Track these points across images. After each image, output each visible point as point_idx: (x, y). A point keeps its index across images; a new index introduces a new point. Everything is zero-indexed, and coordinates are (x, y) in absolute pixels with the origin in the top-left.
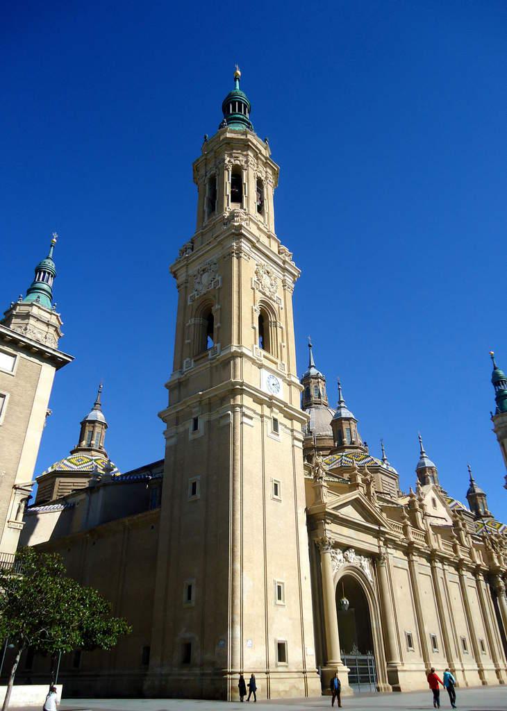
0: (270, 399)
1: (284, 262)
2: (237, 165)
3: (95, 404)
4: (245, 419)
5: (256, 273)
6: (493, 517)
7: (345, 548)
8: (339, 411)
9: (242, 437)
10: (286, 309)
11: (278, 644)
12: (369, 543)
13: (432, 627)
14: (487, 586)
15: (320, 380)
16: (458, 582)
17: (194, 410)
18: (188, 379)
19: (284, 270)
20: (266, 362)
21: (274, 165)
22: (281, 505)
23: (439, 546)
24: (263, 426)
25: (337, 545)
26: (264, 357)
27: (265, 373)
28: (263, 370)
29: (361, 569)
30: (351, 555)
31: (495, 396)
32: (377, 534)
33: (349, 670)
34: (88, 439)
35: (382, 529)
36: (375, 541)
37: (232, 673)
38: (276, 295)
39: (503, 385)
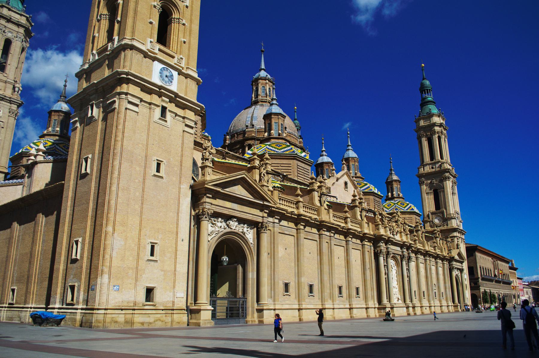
0: (160, 89)
3: (61, 96)
7: (227, 218)
8: (270, 108)
10: (192, 7)
11: (147, 289)
14: (371, 249)
15: (267, 81)
20: (160, 56)
22: (164, 180)
23: (330, 218)
24: (150, 112)
25: (216, 215)
26: (160, 50)
27: (157, 66)
30: (234, 224)
31: (420, 102)
32: (262, 208)
33: (213, 308)
34: (54, 125)
35: (266, 203)
37: (98, 309)
39: (428, 93)
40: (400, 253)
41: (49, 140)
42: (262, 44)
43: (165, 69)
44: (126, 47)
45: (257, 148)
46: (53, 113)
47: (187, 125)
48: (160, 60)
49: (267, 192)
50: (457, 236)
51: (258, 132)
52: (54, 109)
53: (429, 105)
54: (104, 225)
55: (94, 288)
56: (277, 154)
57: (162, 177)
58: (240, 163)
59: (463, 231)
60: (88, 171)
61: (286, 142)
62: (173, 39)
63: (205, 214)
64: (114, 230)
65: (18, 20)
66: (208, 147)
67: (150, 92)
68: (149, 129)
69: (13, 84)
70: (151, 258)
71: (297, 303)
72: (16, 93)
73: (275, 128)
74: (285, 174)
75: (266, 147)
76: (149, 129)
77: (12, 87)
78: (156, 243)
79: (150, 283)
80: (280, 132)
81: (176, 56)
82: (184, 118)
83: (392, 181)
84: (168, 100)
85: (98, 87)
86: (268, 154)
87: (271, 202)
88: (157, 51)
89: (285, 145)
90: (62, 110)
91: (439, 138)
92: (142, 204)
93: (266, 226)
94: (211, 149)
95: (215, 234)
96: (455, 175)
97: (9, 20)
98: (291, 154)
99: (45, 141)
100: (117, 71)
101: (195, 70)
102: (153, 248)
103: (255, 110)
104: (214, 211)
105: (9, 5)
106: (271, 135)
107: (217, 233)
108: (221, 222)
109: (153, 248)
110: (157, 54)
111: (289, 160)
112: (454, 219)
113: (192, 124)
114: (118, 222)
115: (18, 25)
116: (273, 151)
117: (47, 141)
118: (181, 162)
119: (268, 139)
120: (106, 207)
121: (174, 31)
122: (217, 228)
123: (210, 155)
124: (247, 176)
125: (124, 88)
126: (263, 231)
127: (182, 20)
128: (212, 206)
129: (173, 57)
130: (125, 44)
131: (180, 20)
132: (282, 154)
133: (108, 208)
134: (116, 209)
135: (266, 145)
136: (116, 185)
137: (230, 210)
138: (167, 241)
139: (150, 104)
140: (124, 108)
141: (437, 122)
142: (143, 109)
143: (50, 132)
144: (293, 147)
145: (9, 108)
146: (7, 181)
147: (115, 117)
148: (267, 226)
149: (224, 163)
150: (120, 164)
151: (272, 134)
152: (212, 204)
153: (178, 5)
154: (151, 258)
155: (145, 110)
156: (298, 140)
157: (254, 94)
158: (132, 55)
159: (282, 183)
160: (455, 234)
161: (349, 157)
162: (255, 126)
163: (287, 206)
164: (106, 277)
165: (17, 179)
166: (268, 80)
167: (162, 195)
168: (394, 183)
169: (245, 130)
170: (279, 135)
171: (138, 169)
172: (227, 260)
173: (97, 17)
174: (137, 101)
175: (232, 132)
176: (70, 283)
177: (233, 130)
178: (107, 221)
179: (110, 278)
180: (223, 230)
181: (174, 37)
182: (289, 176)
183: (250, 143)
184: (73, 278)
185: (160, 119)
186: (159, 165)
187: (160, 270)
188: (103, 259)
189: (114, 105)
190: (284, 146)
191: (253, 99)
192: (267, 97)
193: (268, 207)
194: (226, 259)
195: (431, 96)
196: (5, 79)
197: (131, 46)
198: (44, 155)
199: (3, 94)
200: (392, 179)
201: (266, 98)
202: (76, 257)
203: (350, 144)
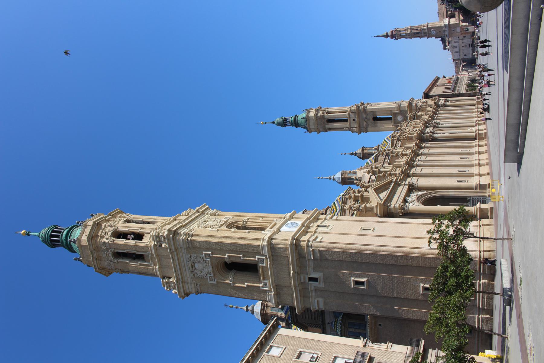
1: (197, 211)
2: (112, 234)
4: (318, 240)
5: (205, 227)
6: (379, 145)
7: (405, 201)
9: (330, 243)
12: (402, 190)
13: (455, 171)
16: (426, 156)
17: (302, 281)
18: (276, 286)
19: (203, 213)
21: (115, 211)
22: (376, 228)
28: (281, 230)
29: (418, 196)
30: (410, 199)
33: (479, 203)
35: (394, 181)
36: (400, 189)
37: (480, 257)
39: (286, 120)
40: (432, 128)
44: (270, 243)
47: (332, 218)
50: (416, 103)
53: (298, 120)
54: (413, 255)
57: (374, 229)
59: (411, 99)
71: (475, 167)
83: (363, 154)
91: (328, 113)
96: (361, 103)
98: (342, 200)
112: (400, 104)
125: (303, 243)
127: (245, 219)
134: (401, 247)
141: (314, 113)
160: (414, 104)
161: (341, 177)
168: (364, 152)
190: (334, 207)
195: (290, 118)
200: (360, 153)
203: (329, 177)
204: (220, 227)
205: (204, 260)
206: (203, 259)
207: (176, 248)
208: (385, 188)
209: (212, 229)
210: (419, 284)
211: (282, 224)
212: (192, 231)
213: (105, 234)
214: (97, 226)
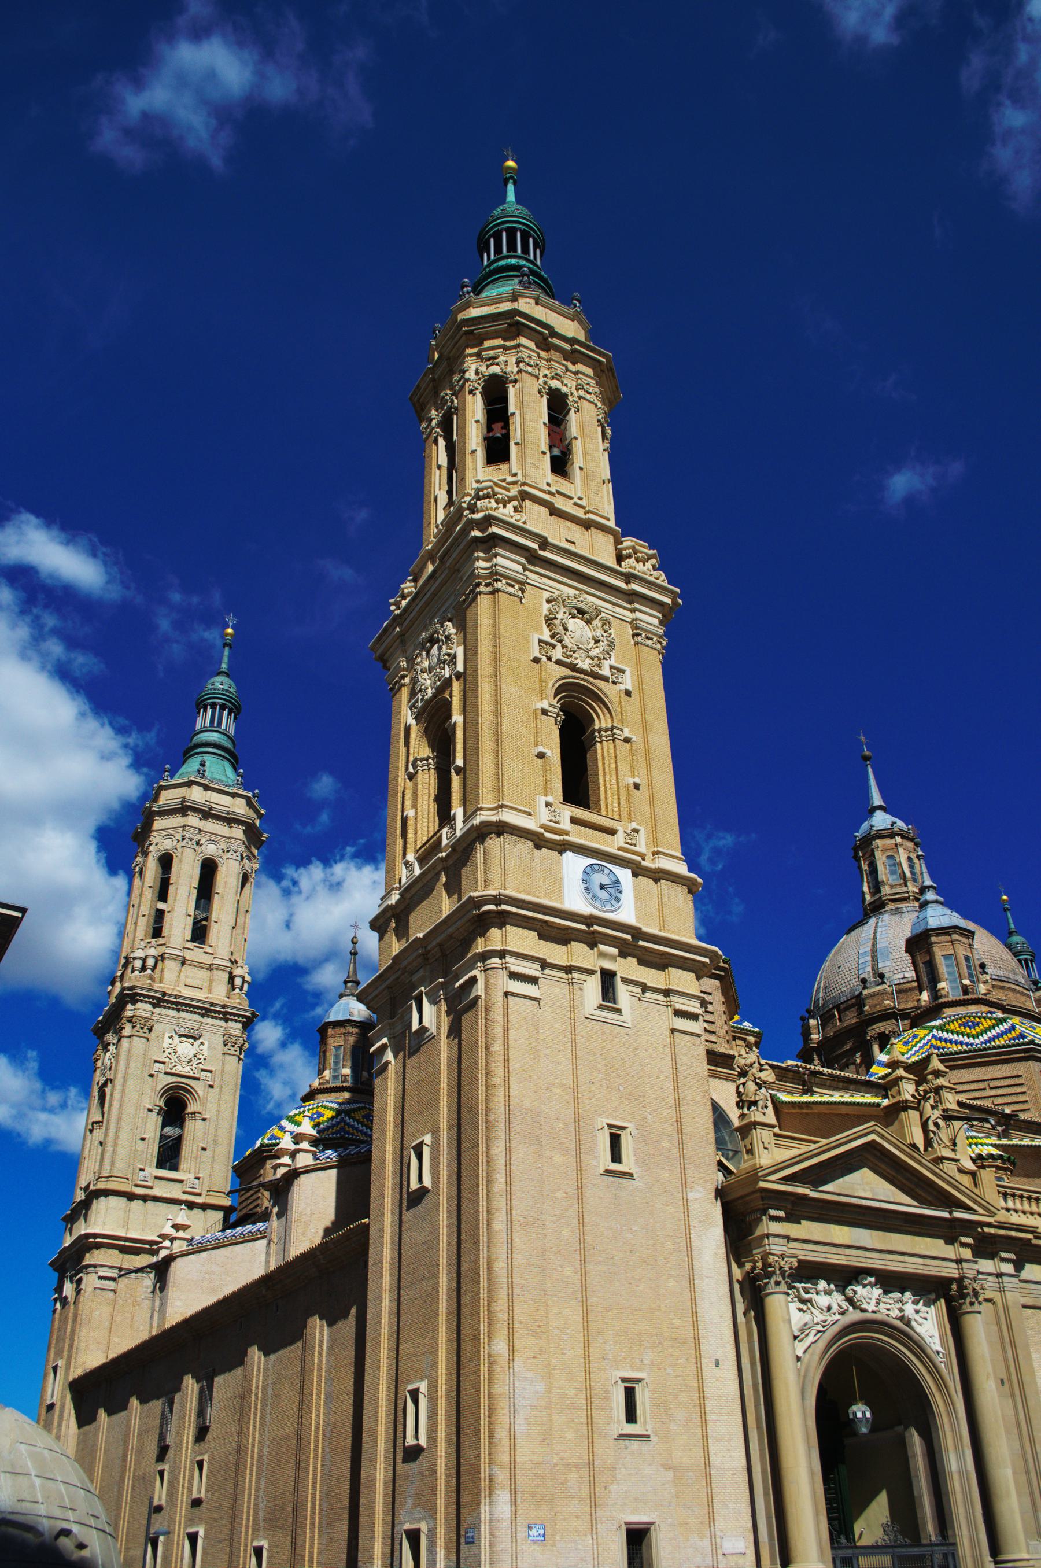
0: (589, 926)
1: (629, 578)
5: (550, 620)
10: (641, 690)
15: (898, 839)
19: (632, 597)
20: (579, 836)
24: (572, 992)
26: (574, 821)
27: (574, 864)
30: (868, 1294)
34: (336, 1063)
35: (958, 1215)
38: (606, 664)
41: (327, 1104)
42: (862, 738)
43: (596, 867)
44: (485, 830)
45: (906, 1043)
46: (330, 1031)
47: (679, 1013)
48: (579, 848)
49: (958, 1177)
51: (899, 992)
52: (333, 1017)
54: (483, 1338)
55: (473, 1537)
56: (970, 1051)
57: (628, 1175)
58: (858, 1098)
60: (427, 1182)
61: (992, 1010)
62: (605, 785)
63: (774, 1272)
64: (512, 1349)
65: (227, 809)
66: (751, 1065)
67: (562, 937)
68: (574, 1042)
69: (229, 969)
70: (630, 1429)
72: (237, 991)
73: (949, 973)
74: (1007, 1111)
75: (934, 1036)
76: (574, 1042)
77: (227, 976)
78: (639, 1381)
79: (635, 1511)
80: (966, 982)
81: (618, 828)
82: (667, 993)
84: (615, 951)
85: (429, 948)
86: (938, 1055)
87: (975, 1207)
88: (566, 825)
89: (990, 1019)
90: (351, 1018)
92: (583, 1261)
93: (974, 1290)
94: (761, 1071)
95: (813, 1332)
97: (207, 814)
98: (1014, 1045)
99: (317, 1107)
100: (471, 898)
101: (678, 854)
102: (630, 1395)
103: (879, 930)
104: (799, 1261)
105: (203, 776)
106: (941, 997)
107: (822, 1329)
108: (828, 1293)
109: (630, 1395)
110: (567, 833)
111: (1012, 1065)
113: (694, 1007)
114: (521, 1323)
115: (229, 820)
116: (956, 1042)
117: (322, 1106)
118: (679, 1121)
119: (934, 1010)
120: (483, 1283)
121: (604, 764)
122: (816, 1312)
123: (760, 1088)
124: (882, 1137)
125: (495, 939)
126: (967, 1307)
127: (621, 730)
128: (792, 1244)
129: (612, 832)
130: (482, 823)
131: (615, 731)
132: (985, 1049)
133: (489, 1284)
134: (511, 1286)
135: (931, 1029)
136: (504, 1213)
137: (848, 1251)
138: (669, 1370)
139: (568, 970)
140: (501, 994)
142: (551, 987)
143: (328, 1082)
144: (1016, 1020)
145: (223, 1032)
146: (230, 1231)
147: (481, 1022)
148: (978, 1288)
149: (808, 1104)
150: (509, 1150)
151: (943, 992)
152: (788, 1239)
153: (604, 694)
154: (630, 1429)
155: (557, 990)
156: (1029, 997)
157: (868, 883)
158: (503, 848)
159: (1004, 1141)
162: (887, 975)
163: (1032, 1214)
164: (503, 1497)
165: (254, 1223)
166: (898, 835)
167: (636, 1228)
169: (861, 993)
170: (965, 990)
171: (558, 1159)
172: (868, 1415)
173: (407, 768)
174: (531, 969)
175: (823, 1005)
176: (405, 1522)
177: (824, 999)
178: (490, 1325)
179: (514, 1503)
180: (838, 1317)
181: (608, 778)
182: (1023, 1116)
183: (882, 1030)
184: (414, 1506)
185: (601, 1007)
186: (615, 1141)
187: (662, 1465)
188: (490, 1443)
189: (474, 990)
190: (986, 1023)
191: (868, 897)
192: (906, 886)
193: (968, 1227)
194: (864, 1414)
196: (208, 960)
197: (498, 826)
198: (313, 1149)
199: (207, 998)
201: (904, 889)
202: (415, 1442)
204: (559, 662)
205: (444, 663)
206: (446, 657)
207: (456, 568)
208: (913, 1186)
209: (540, 641)
210: (426, 1377)
211: (597, 853)
212: (513, 586)
213: (489, 359)
214: (510, 325)
